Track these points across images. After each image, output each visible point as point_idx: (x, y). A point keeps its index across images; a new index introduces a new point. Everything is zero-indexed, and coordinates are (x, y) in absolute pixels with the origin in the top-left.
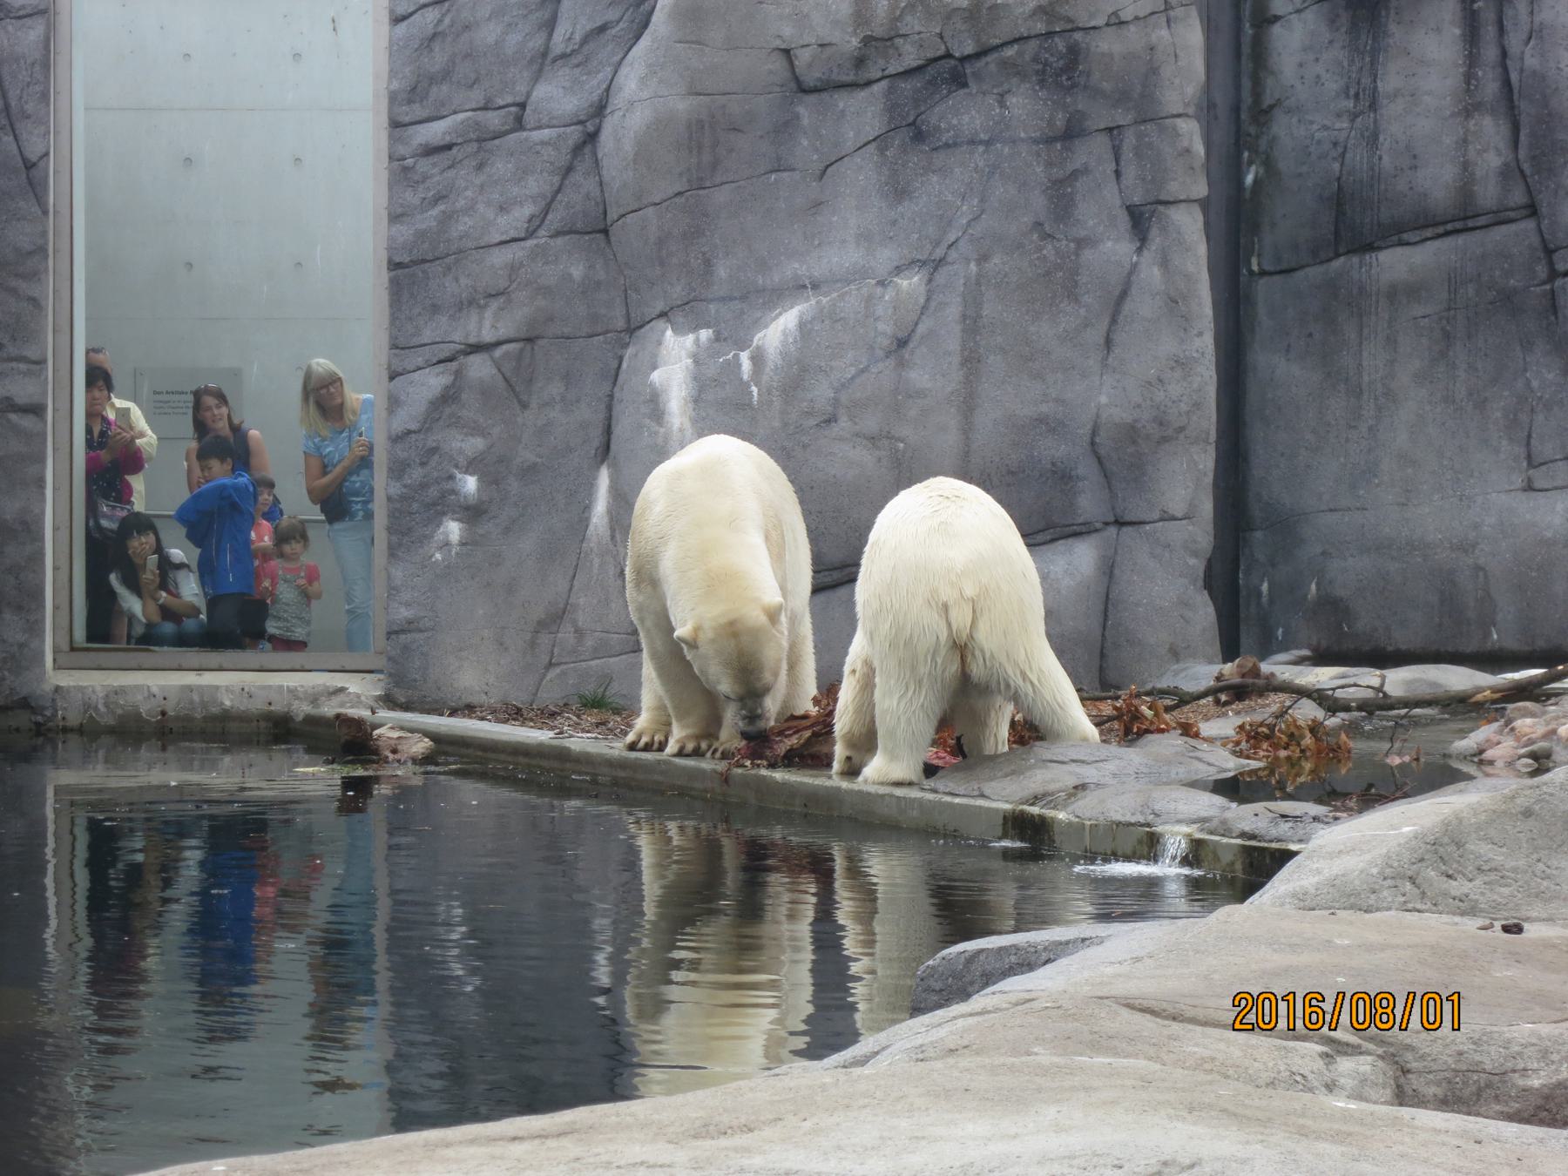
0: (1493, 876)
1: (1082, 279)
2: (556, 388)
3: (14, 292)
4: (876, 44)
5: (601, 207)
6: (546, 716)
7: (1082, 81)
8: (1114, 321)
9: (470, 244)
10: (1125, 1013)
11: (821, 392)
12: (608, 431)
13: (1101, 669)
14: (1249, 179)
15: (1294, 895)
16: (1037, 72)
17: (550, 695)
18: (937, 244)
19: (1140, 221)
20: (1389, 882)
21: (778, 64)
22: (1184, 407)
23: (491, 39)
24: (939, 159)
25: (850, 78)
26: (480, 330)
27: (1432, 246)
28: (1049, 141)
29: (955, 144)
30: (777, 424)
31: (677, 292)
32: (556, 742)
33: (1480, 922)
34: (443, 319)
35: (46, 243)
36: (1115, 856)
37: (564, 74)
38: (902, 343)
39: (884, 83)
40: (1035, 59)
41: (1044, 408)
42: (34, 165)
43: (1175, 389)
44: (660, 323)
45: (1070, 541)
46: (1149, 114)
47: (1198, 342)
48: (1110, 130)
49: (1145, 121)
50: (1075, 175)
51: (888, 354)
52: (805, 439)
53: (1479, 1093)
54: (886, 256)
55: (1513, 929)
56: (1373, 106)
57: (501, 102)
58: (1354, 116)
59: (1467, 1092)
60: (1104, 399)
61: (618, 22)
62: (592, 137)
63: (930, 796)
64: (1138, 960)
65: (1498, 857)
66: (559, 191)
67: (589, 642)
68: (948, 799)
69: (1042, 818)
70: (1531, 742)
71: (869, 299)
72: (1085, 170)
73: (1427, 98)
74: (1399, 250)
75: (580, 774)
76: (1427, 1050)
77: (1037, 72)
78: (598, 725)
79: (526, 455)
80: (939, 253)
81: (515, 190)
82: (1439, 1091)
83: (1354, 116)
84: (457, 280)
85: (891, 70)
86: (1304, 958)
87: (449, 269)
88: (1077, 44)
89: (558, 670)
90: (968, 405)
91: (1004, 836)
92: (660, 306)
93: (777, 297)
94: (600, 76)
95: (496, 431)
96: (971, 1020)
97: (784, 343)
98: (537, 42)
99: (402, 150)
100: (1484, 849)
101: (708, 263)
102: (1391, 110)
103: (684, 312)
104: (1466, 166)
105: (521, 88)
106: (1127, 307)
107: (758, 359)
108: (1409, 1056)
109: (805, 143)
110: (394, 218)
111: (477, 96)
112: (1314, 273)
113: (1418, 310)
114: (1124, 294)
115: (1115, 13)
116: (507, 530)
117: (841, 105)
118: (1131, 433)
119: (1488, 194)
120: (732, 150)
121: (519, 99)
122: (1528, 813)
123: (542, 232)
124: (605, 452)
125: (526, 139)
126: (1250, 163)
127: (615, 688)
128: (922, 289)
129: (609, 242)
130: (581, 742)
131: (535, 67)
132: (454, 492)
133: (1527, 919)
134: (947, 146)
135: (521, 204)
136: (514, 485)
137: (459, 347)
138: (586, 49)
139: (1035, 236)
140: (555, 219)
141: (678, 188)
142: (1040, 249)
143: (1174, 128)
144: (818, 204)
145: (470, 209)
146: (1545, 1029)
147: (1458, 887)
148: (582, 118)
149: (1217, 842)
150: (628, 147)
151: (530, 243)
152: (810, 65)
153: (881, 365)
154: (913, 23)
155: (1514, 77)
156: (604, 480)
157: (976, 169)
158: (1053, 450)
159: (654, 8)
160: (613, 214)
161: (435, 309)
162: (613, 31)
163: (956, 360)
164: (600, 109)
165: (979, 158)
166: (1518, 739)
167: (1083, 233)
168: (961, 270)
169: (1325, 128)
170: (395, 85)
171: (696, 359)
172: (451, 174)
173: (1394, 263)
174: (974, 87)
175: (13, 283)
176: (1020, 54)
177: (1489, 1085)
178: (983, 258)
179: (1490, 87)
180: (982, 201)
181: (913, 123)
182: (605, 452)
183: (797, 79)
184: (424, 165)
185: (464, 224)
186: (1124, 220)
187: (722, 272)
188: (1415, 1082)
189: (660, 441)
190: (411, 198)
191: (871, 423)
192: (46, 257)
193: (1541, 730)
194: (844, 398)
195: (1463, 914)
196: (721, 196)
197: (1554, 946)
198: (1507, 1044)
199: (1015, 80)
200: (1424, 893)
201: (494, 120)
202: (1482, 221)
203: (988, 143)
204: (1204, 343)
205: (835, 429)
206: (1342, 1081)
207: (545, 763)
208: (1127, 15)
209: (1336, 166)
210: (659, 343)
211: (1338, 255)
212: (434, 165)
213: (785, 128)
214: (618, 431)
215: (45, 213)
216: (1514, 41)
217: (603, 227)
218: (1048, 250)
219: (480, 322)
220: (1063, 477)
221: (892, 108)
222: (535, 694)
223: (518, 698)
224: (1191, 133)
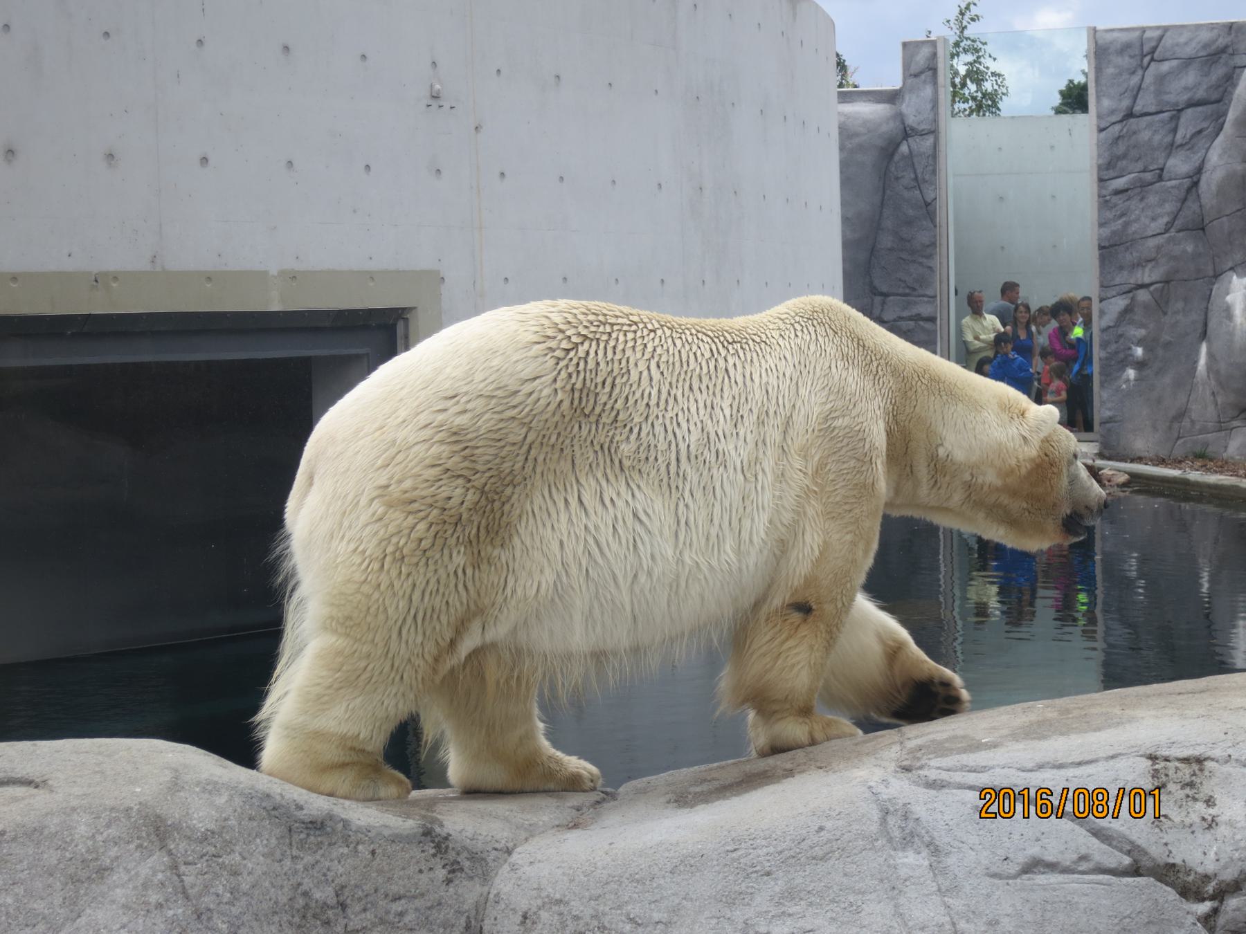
2: (1180, 305)
3: (921, 264)
5: (1201, 217)
6: (1177, 463)
9: (1138, 237)
12: (1206, 324)
17: (1178, 452)
23: (1146, 138)
26: (1143, 278)
32: (1182, 476)
34: (1125, 273)
35: (936, 241)
37: (1182, 153)
42: (930, 204)
44: (1230, 273)
57: (1151, 168)
61: (1208, 128)
62: (1196, 184)
66: (1180, 210)
75: (1194, 491)
78: (1202, 467)
79: (1166, 337)
81: (1159, 210)
84: (1131, 253)
87: (1127, 248)
89: (1182, 440)
92: (1230, 264)
94: (1199, 154)
95: (1152, 326)
98: (1169, 139)
99: (1104, 192)
105: (1161, 161)
110: (1101, 225)
111: (1140, 166)
116: (1157, 374)
121: (1160, 166)
123: (1172, 230)
124: (1204, 335)
125: (1164, 185)
127: (1210, 449)
129: (1205, 234)
130: (1195, 476)
131: (1168, 151)
132: (1132, 355)
136: (1160, 352)
137: (1133, 286)
140: (1178, 223)
141: (1238, 207)
145: (1137, 220)
148: (1191, 174)
150: (1214, 188)
151: (1167, 235)
159: (1224, 121)
160: (1206, 221)
161: (1121, 268)
162: (1205, 133)
164: (1199, 170)
170: (1101, 161)
172: (1127, 203)
175: (921, 260)
182: (1204, 335)
184: (1115, 199)
185: (1134, 227)
189: (1231, 329)
190: (1109, 215)
192: (936, 247)
201: (1148, 176)
207: (1176, 486)
210: (1230, 282)
212: (1120, 199)
215: (935, 226)
217: (1201, 227)
219: (1143, 273)
222: (1171, 452)
223: (1163, 453)
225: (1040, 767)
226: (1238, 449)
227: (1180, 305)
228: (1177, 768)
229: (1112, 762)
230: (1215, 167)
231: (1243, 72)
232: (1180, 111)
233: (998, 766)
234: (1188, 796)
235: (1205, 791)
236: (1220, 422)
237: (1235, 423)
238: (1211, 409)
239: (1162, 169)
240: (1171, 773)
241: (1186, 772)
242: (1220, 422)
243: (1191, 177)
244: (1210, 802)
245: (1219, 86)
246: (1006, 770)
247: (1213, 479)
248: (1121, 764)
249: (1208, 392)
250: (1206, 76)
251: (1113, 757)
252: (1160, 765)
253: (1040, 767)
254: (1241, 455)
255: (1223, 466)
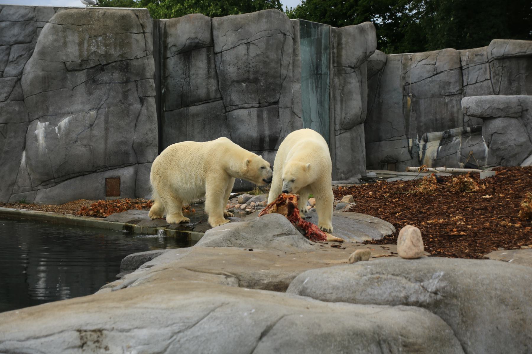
0: (246, 239)
1: (130, 112)
2: (12, 134)
4: (84, 61)
6: (12, 205)
7: (129, 71)
8: (137, 121)
10: (187, 271)
11: (74, 136)
12: (25, 143)
13: (135, 194)
14: (163, 91)
15: (205, 244)
16: (120, 69)
17: (12, 200)
18: (99, 105)
19: (142, 100)
20: (224, 241)
21: (62, 65)
22: (152, 139)
24: (99, 86)
25: (79, 68)
27: (201, 106)
28: (123, 83)
29: (102, 83)
30: (64, 142)
31: (41, 114)
33: (243, 249)
36: (148, 234)
37: (13, 65)
38: (91, 125)
39: (86, 70)
40: (119, 66)
41: (122, 139)
43: (150, 135)
44: (37, 120)
45: (128, 167)
46: (143, 78)
47: (154, 126)
48: (135, 81)
49: (142, 79)
50: (128, 90)
51: (88, 128)
52: (70, 146)
53: (254, 284)
54: (87, 107)
55: (251, 250)
56: (189, 76)
58: (185, 79)
59: (252, 284)
60: (135, 138)
61: (25, 54)
62: (20, 80)
63: (106, 222)
64: (181, 259)
65: (247, 235)
66: (12, 91)
67: (21, 189)
68: (110, 222)
69: (132, 226)
70: (230, 208)
71: (84, 116)
72: (130, 90)
73: (200, 75)
74: (194, 106)
76: (244, 276)
77: (120, 69)
80: (99, 106)
81: (2, 91)
82: (247, 284)
83: (185, 79)
85: (88, 67)
86: (214, 258)
88: (128, 63)
89: (14, 195)
90: (106, 138)
91: (123, 230)
92: (37, 117)
93: (64, 115)
94: (21, 66)
96: (155, 273)
97: (65, 125)
98: (6, 58)
100: (244, 234)
101: (48, 108)
102: (193, 77)
103: (42, 118)
104: (208, 89)
105: (2, 68)
106: (140, 118)
107: (59, 128)
108: (241, 277)
109: (69, 82)
112: (177, 111)
113: (199, 119)
114: (139, 115)
115: (136, 56)
117: (77, 74)
118: (141, 144)
119: (213, 95)
120: (52, 83)
121: (2, 70)
122: (252, 227)
123: (8, 100)
124: (24, 148)
126: (163, 88)
127: (27, 199)
128: (96, 114)
129: (24, 103)
130: (23, 211)
133: (254, 248)
134: (100, 84)
135: (3, 94)
138: (17, 60)
139: (120, 103)
140: (11, 97)
141: (40, 91)
142: (121, 106)
143: (149, 81)
144: (72, 96)
146: (266, 271)
147: (238, 242)
149: (170, 231)
150: (28, 82)
151: (6, 102)
152: (70, 66)
153: (87, 130)
154: (93, 57)
155: (218, 71)
156: (24, 154)
157: (107, 89)
158: (124, 148)
159: (33, 52)
160: (25, 97)
162: (24, 56)
163: (103, 129)
164: (21, 73)
165: (107, 86)
166: (227, 208)
167: (130, 103)
168: (104, 110)
169: (179, 81)
171: (45, 128)
173: (194, 109)
174: (106, 71)
176: (116, 64)
177: (256, 283)
178: (109, 108)
179: (213, 73)
180: (108, 95)
181: (93, 79)
182: (24, 148)
183: (66, 68)
186: (138, 99)
187: (51, 110)
188: (242, 282)
189: (37, 146)
191: (85, 142)
193: (231, 206)
194: (79, 137)
195: (240, 247)
196: (50, 93)
197: (260, 254)
198: (259, 274)
199: (115, 70)
200: (232, 243)
202: (211, 101)
203: (109, 83)
204: (156, 126)
205: (77, 144)
206: (230, 283)
208: (138, 57)
209: (181, 89)
211: (182, 107)
213: (64, 79)
214: (27, 143)
216: (218, 64)
218: (123, 106)
220: (126, 153)
221: (88, 75)
223: (4, 201)
224: (152, 81)
225: (28, 339)
226: (41, 199)
227: (12, 134)
228: (91, 335)
229: (61, 334)
230: (29, 73)
231: (41, 30)
232: (11, 45)
233: (7, 340)
234: (97, 347)
235: (104, 343)
236: (32, 187)
237: (39, 187)
238: (28, 181)
239: (3, 72)
240: (88, 337)
241: (95, 336)
242: (32, 187)
243: (17, 76)
244: (106, 348)
245: (30, 36)
246: (11, 342)
247: (32, 212)
248: (66, 335)
249: (26, 174)
250: (23, 30)
251: (62, 332)
252: (83, 334)
253: (28, 339)
254: (42, 201)
255: (35, 206)
